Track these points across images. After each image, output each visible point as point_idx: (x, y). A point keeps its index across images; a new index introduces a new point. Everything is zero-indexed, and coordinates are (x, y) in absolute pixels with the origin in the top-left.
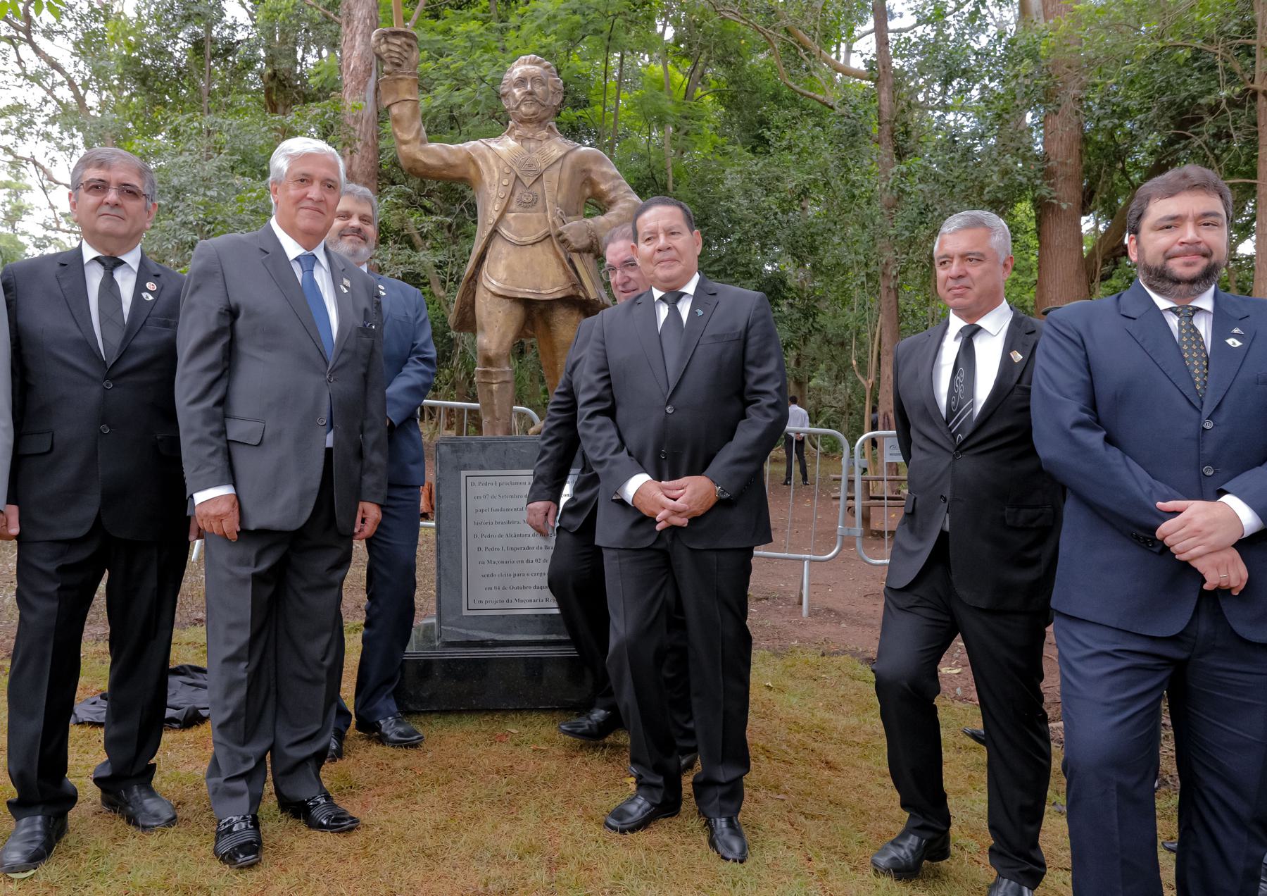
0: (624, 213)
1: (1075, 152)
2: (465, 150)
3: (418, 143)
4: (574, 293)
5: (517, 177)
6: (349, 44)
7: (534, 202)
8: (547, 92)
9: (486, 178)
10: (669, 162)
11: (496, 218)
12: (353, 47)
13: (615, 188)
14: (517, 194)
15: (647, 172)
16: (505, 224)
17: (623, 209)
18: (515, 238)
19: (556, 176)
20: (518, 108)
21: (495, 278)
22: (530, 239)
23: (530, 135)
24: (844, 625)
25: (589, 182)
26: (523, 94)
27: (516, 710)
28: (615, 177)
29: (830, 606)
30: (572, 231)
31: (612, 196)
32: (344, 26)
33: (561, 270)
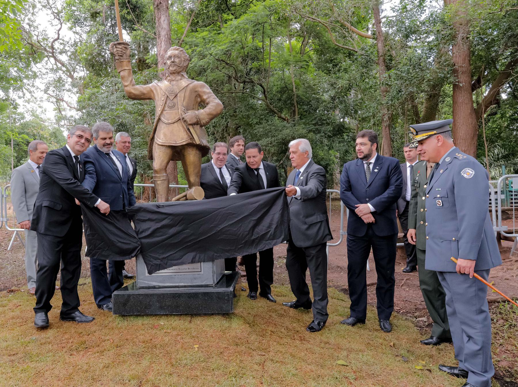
0: (212, 107)
1: (467, 61)
2: (149, 87)
3: (131, 86)
4: (191, 142)
5: (167, 96)
6: (159, 46)
7: (174, 106)
8: (181, 61)
9: (156, 98)
10: (293, 80)
11: (159, 113)
12: (161, 47)
13: (209, 98)
14: (168, 103)
15: (284, 85)
16: (163, 116)
17: (212, 106)
18: (166, 121)
19: (183, 95)
20: (169, 68)
21: (160, 139)
22: (174, 121)
23: (174, 79)
24: (342, 273)
25: (199, 96)
26: (170, 62)
27: (167, 315)
28: (210, 93)
29: (339, 265)
30: (188, 117)
31: (208, 100)
32: (158, 39)
33: (185, 133)
